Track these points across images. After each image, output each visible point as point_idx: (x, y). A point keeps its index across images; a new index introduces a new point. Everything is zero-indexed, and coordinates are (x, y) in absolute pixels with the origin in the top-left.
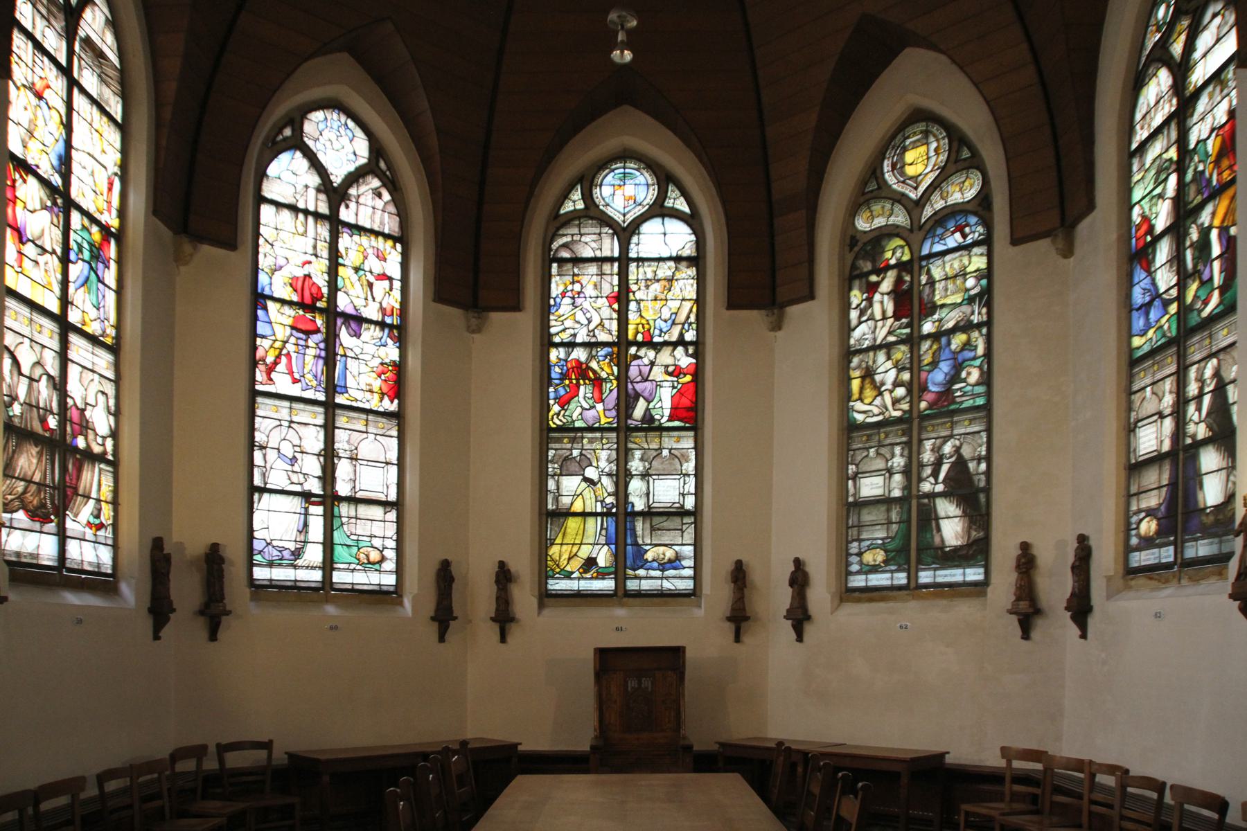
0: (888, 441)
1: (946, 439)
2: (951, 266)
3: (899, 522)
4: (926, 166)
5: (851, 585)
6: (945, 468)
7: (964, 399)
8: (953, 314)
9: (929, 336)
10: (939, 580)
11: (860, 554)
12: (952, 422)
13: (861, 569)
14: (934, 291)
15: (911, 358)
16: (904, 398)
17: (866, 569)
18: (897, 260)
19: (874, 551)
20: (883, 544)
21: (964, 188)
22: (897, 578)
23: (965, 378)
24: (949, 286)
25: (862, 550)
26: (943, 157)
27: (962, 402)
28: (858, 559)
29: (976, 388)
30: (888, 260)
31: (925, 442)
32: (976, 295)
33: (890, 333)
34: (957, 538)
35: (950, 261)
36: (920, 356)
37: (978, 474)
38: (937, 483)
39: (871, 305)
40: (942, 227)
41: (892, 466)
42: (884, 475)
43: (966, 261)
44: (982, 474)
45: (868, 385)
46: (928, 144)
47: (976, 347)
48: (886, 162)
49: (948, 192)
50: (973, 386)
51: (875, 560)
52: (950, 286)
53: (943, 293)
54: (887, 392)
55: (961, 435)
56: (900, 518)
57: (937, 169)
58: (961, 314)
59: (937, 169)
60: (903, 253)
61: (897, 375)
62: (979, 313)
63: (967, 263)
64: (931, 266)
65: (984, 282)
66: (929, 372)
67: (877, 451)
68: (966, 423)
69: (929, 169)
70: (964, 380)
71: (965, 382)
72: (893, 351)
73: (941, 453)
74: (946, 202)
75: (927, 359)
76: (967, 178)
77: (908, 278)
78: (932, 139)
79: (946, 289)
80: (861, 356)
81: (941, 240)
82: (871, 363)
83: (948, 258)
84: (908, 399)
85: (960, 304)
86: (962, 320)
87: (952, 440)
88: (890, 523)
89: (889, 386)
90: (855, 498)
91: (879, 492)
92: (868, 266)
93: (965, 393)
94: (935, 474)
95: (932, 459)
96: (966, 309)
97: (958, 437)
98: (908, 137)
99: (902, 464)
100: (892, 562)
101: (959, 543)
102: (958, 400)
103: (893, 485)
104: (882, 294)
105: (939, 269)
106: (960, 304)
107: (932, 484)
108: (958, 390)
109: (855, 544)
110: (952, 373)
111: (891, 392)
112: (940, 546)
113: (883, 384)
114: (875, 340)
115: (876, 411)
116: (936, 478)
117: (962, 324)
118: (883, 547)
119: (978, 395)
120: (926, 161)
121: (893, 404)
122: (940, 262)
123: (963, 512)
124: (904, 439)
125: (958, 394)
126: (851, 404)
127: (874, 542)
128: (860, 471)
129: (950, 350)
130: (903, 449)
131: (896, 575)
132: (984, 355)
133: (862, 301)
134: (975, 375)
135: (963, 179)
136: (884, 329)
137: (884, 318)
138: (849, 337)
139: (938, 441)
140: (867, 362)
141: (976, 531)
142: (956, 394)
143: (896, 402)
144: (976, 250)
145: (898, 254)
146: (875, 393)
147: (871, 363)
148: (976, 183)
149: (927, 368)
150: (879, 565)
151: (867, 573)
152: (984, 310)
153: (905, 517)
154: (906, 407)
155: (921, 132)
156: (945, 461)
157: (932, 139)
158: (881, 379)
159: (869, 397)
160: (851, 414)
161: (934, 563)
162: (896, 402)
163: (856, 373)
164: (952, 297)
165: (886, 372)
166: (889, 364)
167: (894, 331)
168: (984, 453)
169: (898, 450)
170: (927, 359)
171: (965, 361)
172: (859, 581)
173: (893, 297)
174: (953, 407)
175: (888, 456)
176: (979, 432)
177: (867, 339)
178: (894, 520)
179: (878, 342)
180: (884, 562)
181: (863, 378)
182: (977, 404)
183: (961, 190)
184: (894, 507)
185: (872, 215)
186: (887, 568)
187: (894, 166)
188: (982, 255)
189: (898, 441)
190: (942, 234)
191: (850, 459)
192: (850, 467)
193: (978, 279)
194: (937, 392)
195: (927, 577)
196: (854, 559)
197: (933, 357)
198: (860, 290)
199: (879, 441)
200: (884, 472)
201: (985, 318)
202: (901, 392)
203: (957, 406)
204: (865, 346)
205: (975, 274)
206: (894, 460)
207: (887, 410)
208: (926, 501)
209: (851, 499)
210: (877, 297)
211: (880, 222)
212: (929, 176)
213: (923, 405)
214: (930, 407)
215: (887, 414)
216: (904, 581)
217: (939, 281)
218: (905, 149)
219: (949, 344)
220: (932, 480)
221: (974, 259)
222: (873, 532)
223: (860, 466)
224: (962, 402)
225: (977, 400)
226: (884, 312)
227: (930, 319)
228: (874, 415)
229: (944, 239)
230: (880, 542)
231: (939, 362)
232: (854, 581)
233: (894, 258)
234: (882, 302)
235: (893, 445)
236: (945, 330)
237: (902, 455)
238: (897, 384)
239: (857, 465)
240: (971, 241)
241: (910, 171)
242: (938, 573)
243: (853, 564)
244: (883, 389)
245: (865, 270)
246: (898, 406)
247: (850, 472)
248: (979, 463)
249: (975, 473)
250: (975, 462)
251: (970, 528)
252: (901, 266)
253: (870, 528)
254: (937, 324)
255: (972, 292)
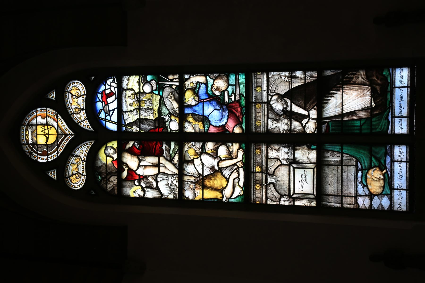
0: (264, 163)
1: (270, 108)
2: (131, 105)
3: (342, 153)
4: (53, 126)
5: (404, 208)
6: (296, 109)
7: (238, 93)
8: (168, 103)
9: (181, 125)
10: (405, 112)
11: (371, 196)
12: (256, 103)
13: (387, 195)
14: (146, 120)
15: (195, 141)
16: (228, 148)
17: (387, 191)
18: (115, 153)
19: (369, 180)
20: (362, 170)
21: (76, 95)
22: (400, 156)
23: (221, 92)
24: (146, 107)
25: (367, 193)
26: (51, 112)
27: (241, 94)
28: (376, 198)
29: (231, 83)
30: (113, 161)
31: (269, 128)
32: (157, 84)
33: (171, 160)
34: (363, 96)
35: (127, 106)
36: (195, 133)
37: (305, 78)
38: (308, 117)
39: (145, 177)
40: (100, 113)
41: (287, 160)
42: (294, 168)
43: (129, 93)
44: (305, 75)
45: (211, 181)
46: (37, 125)
47: (198, 83)
48: (40, 160)
49: (76, 108)
50: (228, 85)
51: (380, 179)
52: (146, 106)
53: (150, 113)
54: (220, 164)
55: (268, 95)
56: (338, 152)
57: (57, 117)
58: (169, 97)
59: (57, 117)
60: (112, 147)
61: (208, 154)
62: (172, 81)
63: (132, 92)
64: (127, 123)
65: (149, 78)
66: (210, 125)
67: (270, 175)
68: (258, 90)
69: (55, 124)
70: (223, 92)
71: (224, 92)
72: (188, 158)
73: (282, 113)
74: (83, 109)
75: (199, 126)
76: (70, 92)
77: (131, 144)
78: (34, 122)
79: (148, 109)
80: (185, 189)
81: (109, 115)
82: (192, 179)
83: (125, 109)
84: (230, 144)
85: (162, 97)
86: (174, 95)
87: (272, 103)
88: (341, 164)
89: (214, 162)
90: (312, 199)
91: (310, 173)
92: (114, 180)
93: (233, 92)
94: (299, 118)
95: (286, 121)
96: (167, 91)
97: (270, 97)
98: (27, 141)
99: (286, 150)
100: (383, 161)
101: (369, 93)
102: (238, 98)
103: (305, 160)
104: (139, 166)
105: (130, 116)
106: (162, 97)
107: (308, 121)
108: (229, 99)
109: (360, 200)
110: (214, 103)
111: (221, 160)
112: (369, 111)
113: (212, 168)
114: (175, 174)
115: (235, 175)
116: (304, 117)
117: (177, 95)
118: (365, 171)
119: (237, 80)
120: (49, 127)
121: (232, 158)
122: (126, 115)
123: (338, 90)
124: (264, 148)
125: (233, 98)
126: (224, 199)
127: (360, 180)
128: (287, 194)
129: (195, 105)
130: (272, 149)
131: (396, 158)
132: (206, 76)
133: (139, 185)
134: (221, 84)
135: (70, 95)
136: (166, 166)
137: (158, 165)
138: (167, 200)
139: (270, 116)
140: (191, 182)
141: (358, 78)
142: (233, 100)
143: (230, 156)
144: (124, 86)
145: (110, 151)
146: (219, 176)
147: (192, 179)
148: (75, 85)
149: (206, 126)
150: (384, 175)
151: (392, 189)
152: (171, 77)
153: (337, 148)
154: (236, 146)
155: (27, 130)
156: (289, 109)
157: (34, 122)
158: (208, 170)
159: (221, 182)
160: (233, 200)
161: (387, 118)
162: (230, 156)
163: (199, 192)
164: (155, 105)
165: (203, 164)
166: (197, 162)
167: (171, 155)
168: (287, 74)
169: (273, 154)
170: (199, 126)
171: (207, 93)
172: (400, 198)
173: (143, 157)
174: (243, 103)
175: (278, 163)
176: (268, 78)
177: (172, 182)
178: (339, 159)
179: (176, 171)
180: (381, 170)
181: (204, 187)
182: (244, 80)
183: (77, 97)
184: (326, 159)
185: (75, 174)
186: (388, 166)
187: (45, 154)
188: (128, 80)
189: (265, 154)
190: (106, 113)
191: (275, 203)
192: (282, 203)
193: (146, 82)
194: (228, 117)
195: (401, 125)
196: (376, 202)
197: (199, 122)
198: (131, 187)
199: (262, 172)
200: (292, 168)
201: (176, 77)
202: (222, 151)
203: (243, 99)
204: (177, 184)
205: (142, 86)
206: (281, 158)
207: (235, 164)
208: (324, 126)
209: (314, 204)
210: (140, 172)
211: (82, 168)
212: (60, 123)
213: (237, 130)
214: (239, 123)
215: (240, 164)
216: (404, 149)
217: (140, 116)
218: (35, 144)
219: (190, 106)
220: (304, 122)
221: (130, 87)
222: (349, 181)
223: (283, 193)
224: (241, 94)
225: (241, 81)
226: (153, 165)
227: (167, 124)
228: (238, 177)
229: (110, 111)
230: (360, 174)
231: (203, 116)
232: (400, 204)
233: (113, 156)
234: (145, 166)
235: (267, 158)
236: (179, 110)
237: (278, 150)
238: (215, 155)
239: (282, 196)
240: (116, 89)
241: (52, 139)
242: (397, 113)
243: (381, 204)
244: (217, 168)
245: (116, 182)
246: (234, 154)
247: (287, 203)
248: (296, 77)
249: (303, 81)
250: (294, 81)
251: (355, 84)
252: (120, 151)
253: (345, 184)
254: (173, 118)
255: (155, 88)
